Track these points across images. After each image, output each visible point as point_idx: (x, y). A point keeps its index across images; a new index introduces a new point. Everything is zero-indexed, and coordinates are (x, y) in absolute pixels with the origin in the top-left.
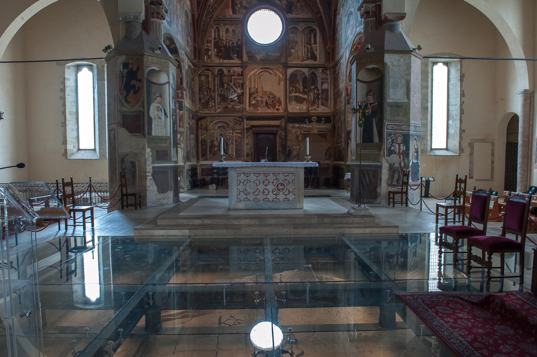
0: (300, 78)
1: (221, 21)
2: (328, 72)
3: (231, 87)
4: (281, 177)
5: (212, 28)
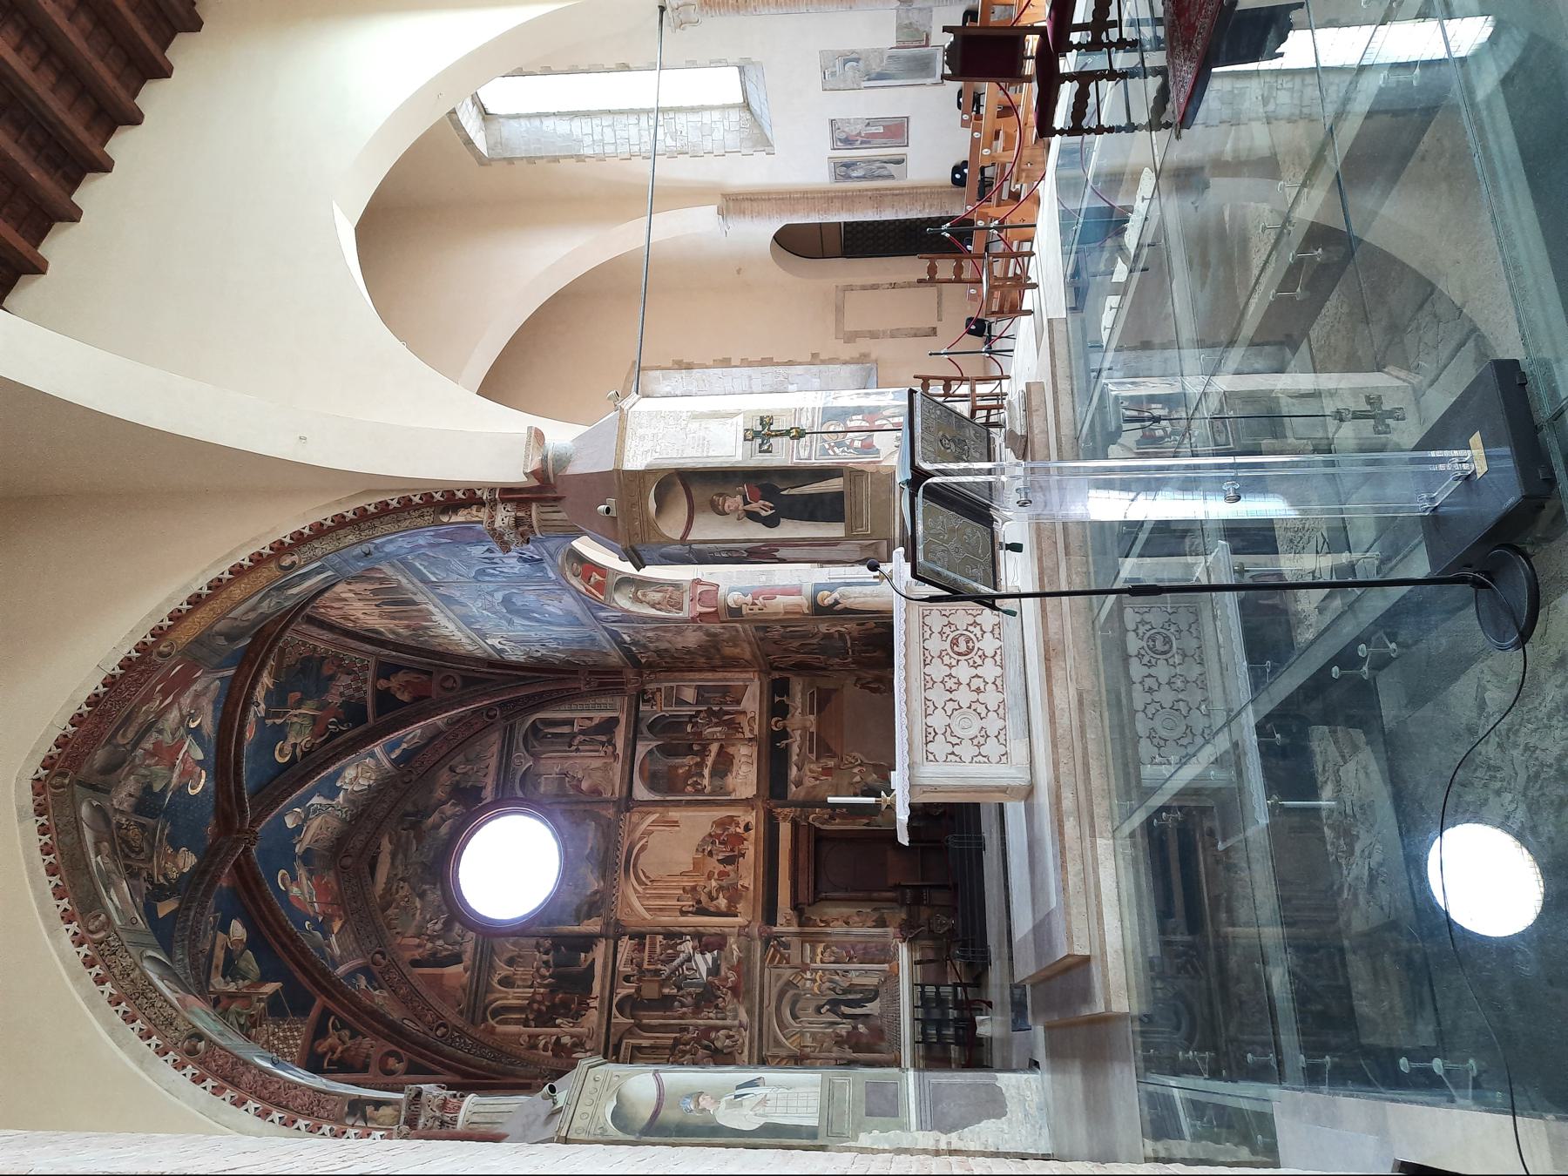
0: (663, 763)
1: (477, 1005)
2: (652, 686)
3: (673, 972)
4: (935, 645)
5: (492, 1031)
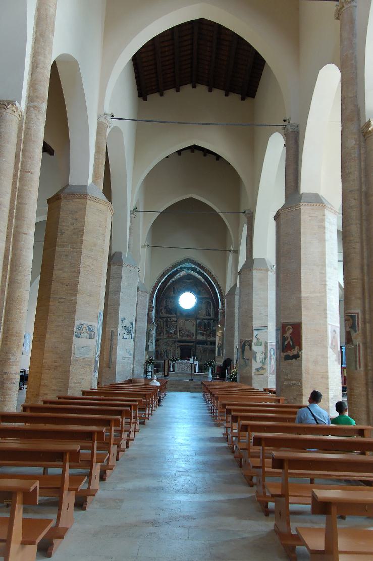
0: (203, 324)
